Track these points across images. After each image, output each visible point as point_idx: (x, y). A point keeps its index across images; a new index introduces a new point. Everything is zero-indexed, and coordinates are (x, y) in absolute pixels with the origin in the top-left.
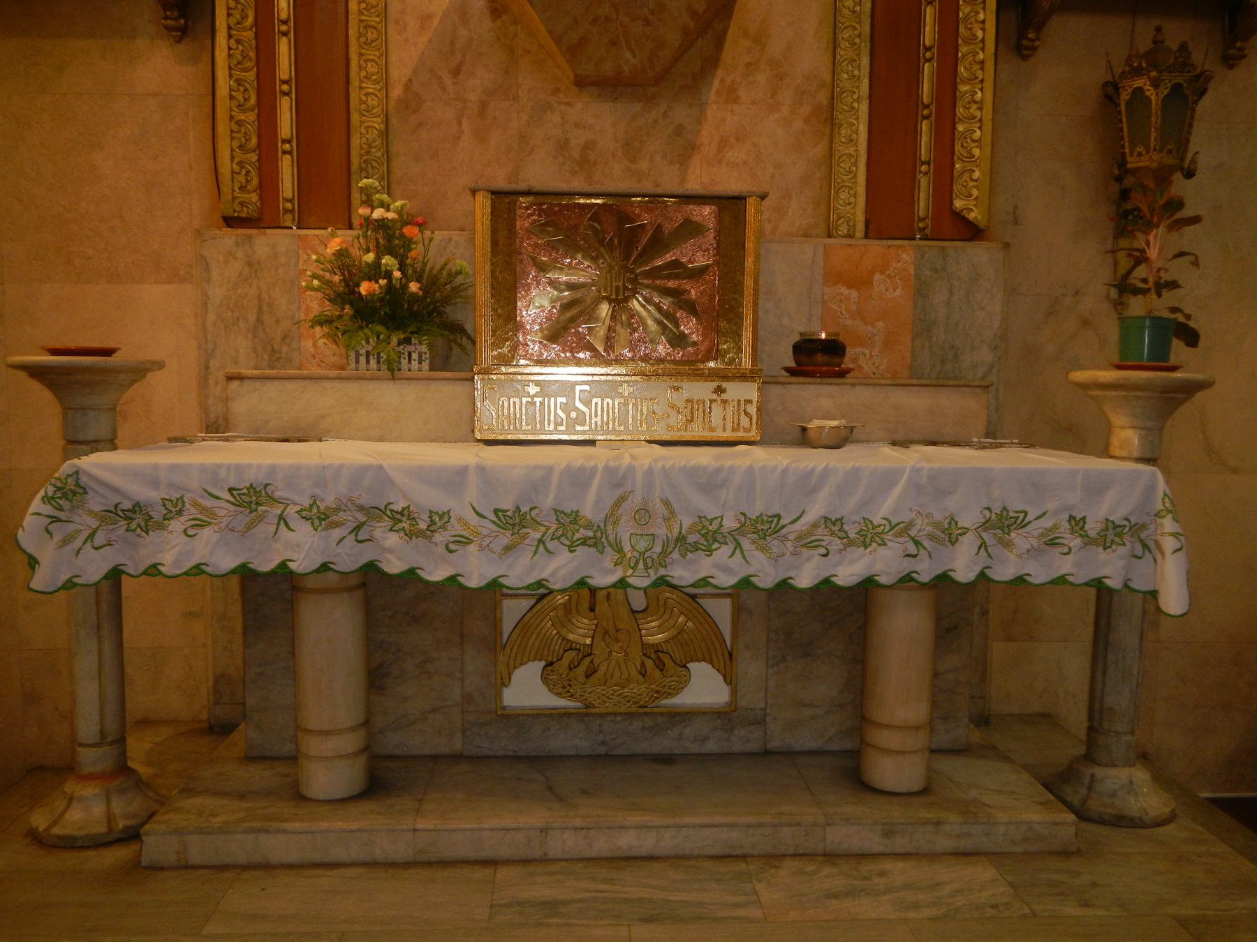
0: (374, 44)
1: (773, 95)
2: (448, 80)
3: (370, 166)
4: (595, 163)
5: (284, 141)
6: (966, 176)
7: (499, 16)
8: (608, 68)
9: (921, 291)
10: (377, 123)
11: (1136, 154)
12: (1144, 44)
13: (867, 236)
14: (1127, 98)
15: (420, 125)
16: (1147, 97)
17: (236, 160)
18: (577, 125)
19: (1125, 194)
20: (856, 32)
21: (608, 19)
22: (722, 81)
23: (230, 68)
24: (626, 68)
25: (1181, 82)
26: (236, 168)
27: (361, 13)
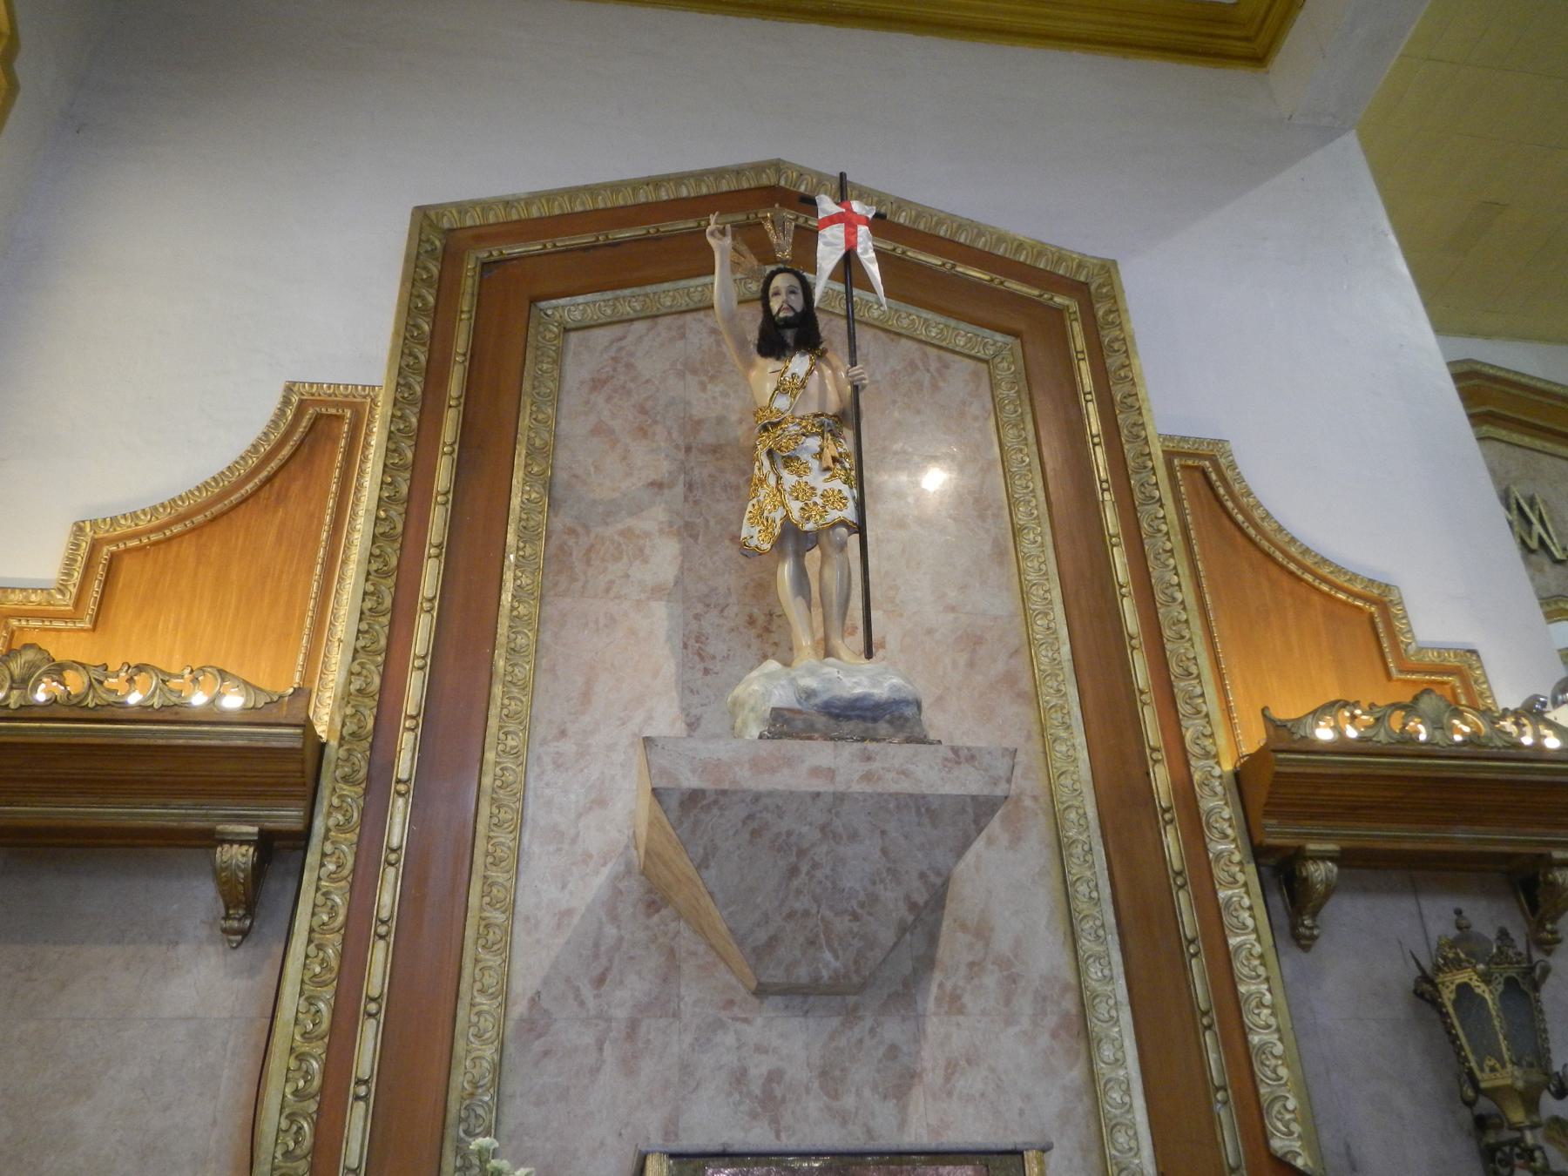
0: (495, 947)
1: (1008, 1002)
2: (587, 992)
3: (472, 1115)
4: (784, 1100)
5: (359, 1082)
6: (1277, 1106)
7: (658, 911)
8: (803, 974)
10: (489, 1052)
11: (1487, 1069)
14: (1453, 996)
15: (546, 1053)
16: (1478, 995)
17: (287, 1111)
18: (760, 1049)
19: (1481, 1123)
20: (1098, 923)
21: (806, 913)
22: (941, 986)
23: (303, 981)
24: (825, 974)
25: (1514, 975)
26: (284, 1124)
27: (482, 909)
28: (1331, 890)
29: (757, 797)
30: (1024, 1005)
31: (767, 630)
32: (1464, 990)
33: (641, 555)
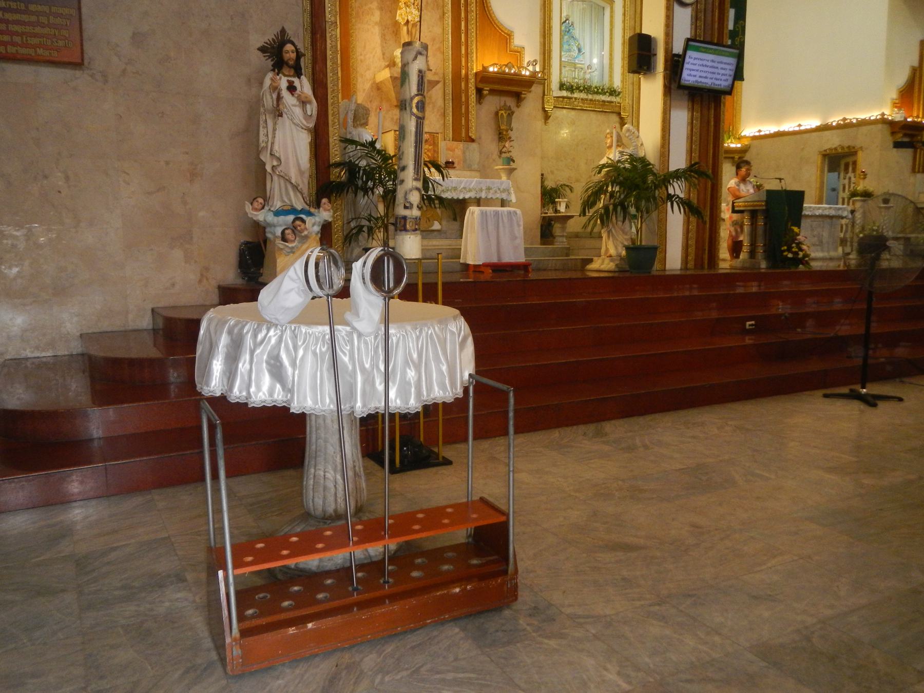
9: (464, 153)
12: (502, 104)
13: (454, 139)
19: (500, 134)
28: (486, 95)
30: (436, 110)
31: (396, 34)
32: (502, 114)
33: (373, 14)
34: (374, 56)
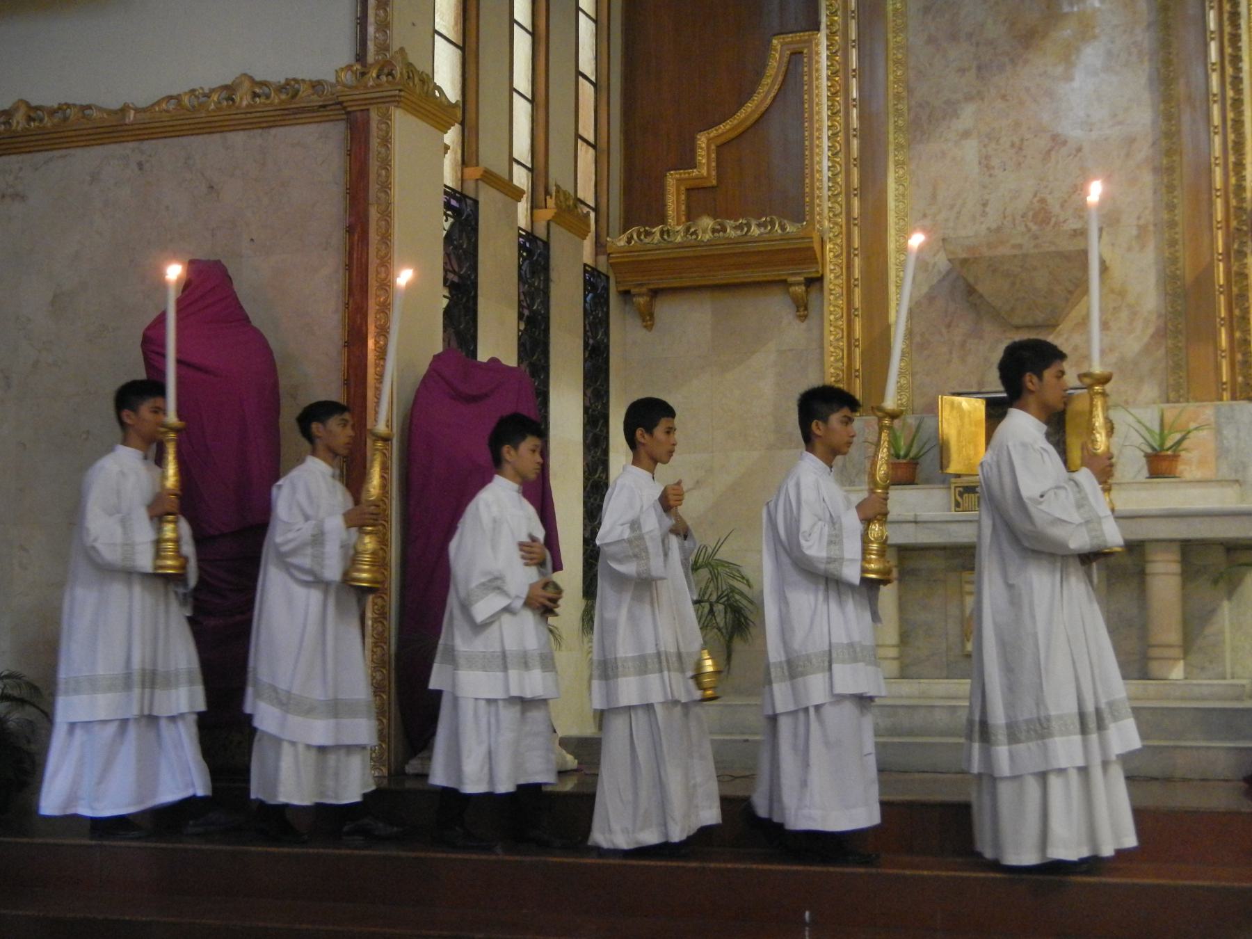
2: (944, 330)
29: (990, 259)
31: (1021, 149)
34: (959, 213)
